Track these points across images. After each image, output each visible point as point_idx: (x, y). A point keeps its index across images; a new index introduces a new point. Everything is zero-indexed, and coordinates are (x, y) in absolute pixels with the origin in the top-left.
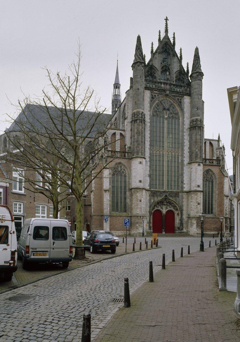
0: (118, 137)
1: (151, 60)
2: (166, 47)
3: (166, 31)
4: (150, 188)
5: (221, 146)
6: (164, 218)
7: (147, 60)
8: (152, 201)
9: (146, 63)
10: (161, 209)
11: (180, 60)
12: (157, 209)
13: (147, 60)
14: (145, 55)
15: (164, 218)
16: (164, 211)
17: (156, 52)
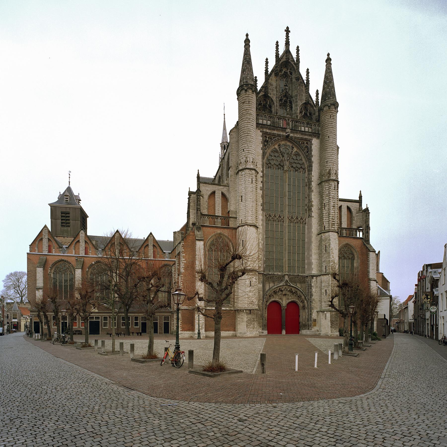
0: (218, 196)
1: (265, 87)
2: (286, 66)
3: (287, 43)
4: (264, 271)
5: (364, 207)
6: (284, 312)
7: (260, 83)
8: (267, 288)
9: (259, 88)
10: (280, 301)
11: (307, 85)
12: (273, 299)
13: (260, 83)
14: (256, 77)
15: (284, 312)
16: (284, 302)
17: (271, 74)
